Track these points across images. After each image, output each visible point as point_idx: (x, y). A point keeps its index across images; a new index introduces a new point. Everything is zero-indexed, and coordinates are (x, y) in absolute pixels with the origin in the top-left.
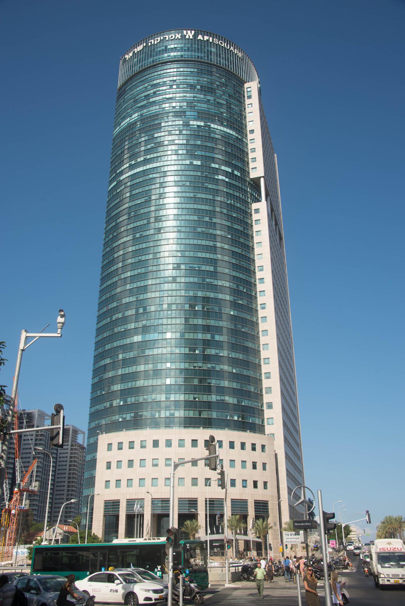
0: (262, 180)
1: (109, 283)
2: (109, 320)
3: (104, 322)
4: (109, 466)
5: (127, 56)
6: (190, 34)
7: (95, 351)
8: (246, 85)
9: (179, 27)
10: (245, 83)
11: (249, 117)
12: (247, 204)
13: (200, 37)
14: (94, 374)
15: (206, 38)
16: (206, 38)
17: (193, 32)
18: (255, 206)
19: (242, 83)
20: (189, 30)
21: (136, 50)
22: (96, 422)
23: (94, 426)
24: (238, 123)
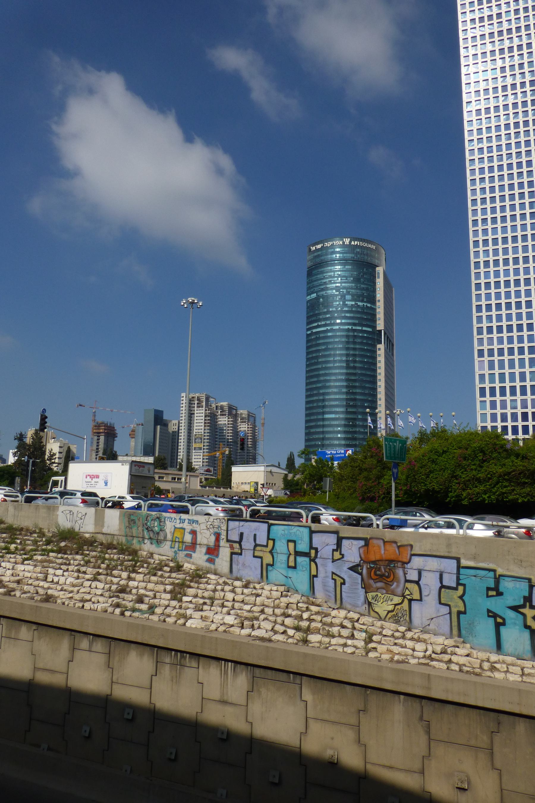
0: (383, 331)
6: (347, 241)
8: (377, 269)
9: (341, 238)
11: (378, 289)
12: (375, 346)
13: (353, 243)
15: (356, 243)
18: (379, 346)
19: (374, 267)
24: (372, 300)
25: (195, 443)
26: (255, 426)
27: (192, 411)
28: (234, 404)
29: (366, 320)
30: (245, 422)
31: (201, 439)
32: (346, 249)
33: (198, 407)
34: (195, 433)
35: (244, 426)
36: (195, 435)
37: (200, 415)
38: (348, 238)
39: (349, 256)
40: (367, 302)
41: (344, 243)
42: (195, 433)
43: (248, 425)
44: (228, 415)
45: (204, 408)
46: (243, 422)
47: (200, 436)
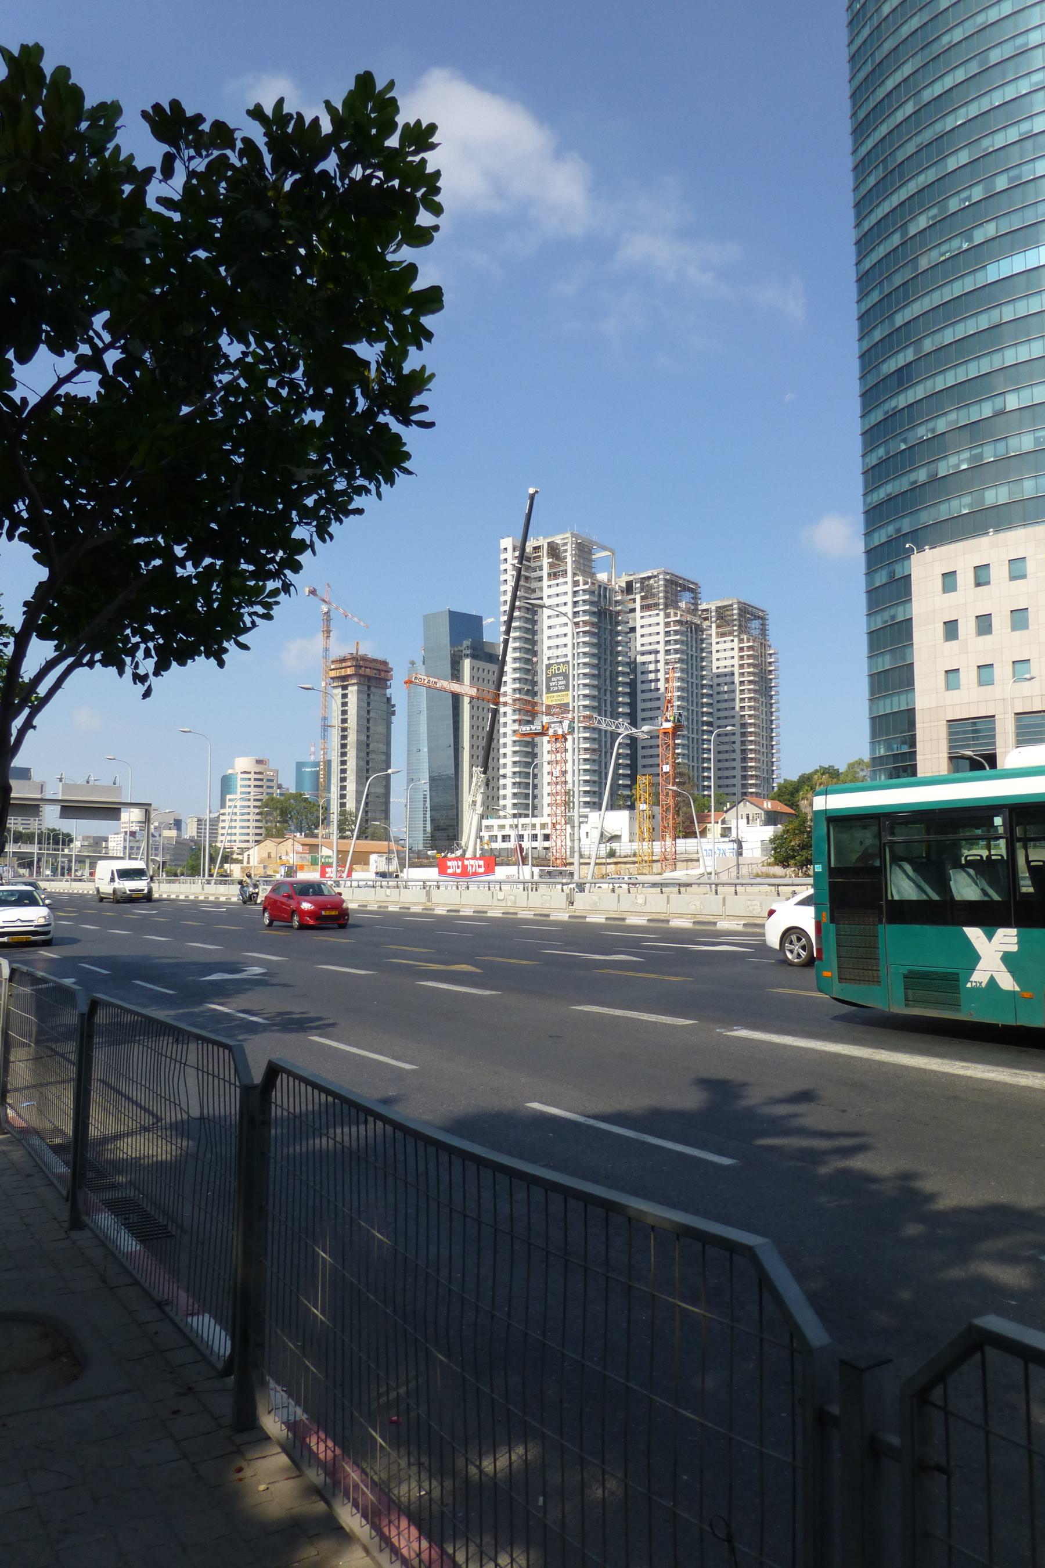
1: (884, 130)
2: (896, 239)
3: (881, 251)
4: (951, 629)
7: (860, 339)
14: (864, 405)
22: (891, 529)
23: (884, 539)
25: (549, 691)
26: (764, 646)
27: (534, 591)
28: (687, 572)
30: (731, 633)
31: (566, 676)
33: (553, 575)
34: (546, 662)
35: (729, 645)
36: (548, 666)
37: (560, 602)
42: (546, 662)
43: (741, 641)
44: (666, 606)
45: (569, 578)
46: (723, 635)
47: (563, 668)
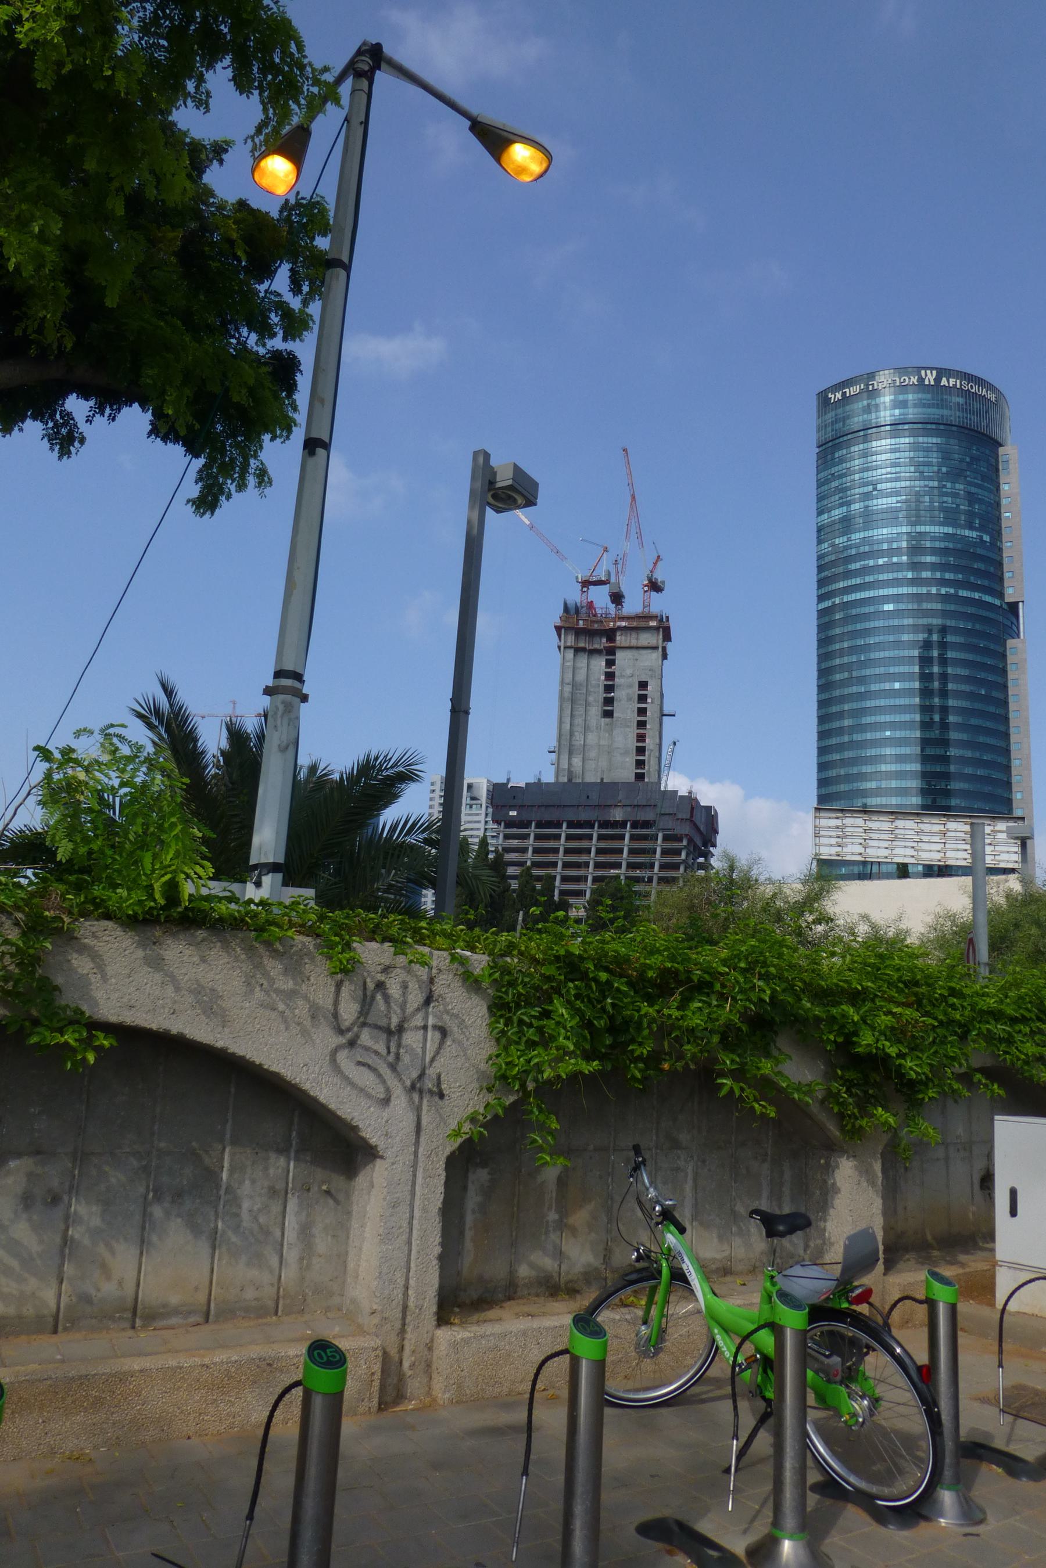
5: (830, 395)
10: (1001, 445)
15: (952, 381)
16: (952, 381)
17: (934, 372)
20: (928, 368)
21: (847, 390)
29: (979, 573)
32: (929, 396)
38: (932, 369)
39: (935, 413)
40: (982, 528)
41: (921, 380)
